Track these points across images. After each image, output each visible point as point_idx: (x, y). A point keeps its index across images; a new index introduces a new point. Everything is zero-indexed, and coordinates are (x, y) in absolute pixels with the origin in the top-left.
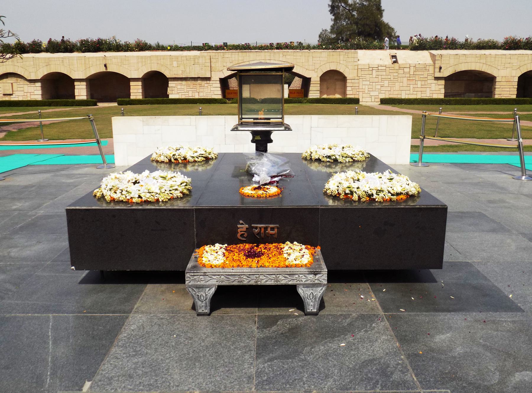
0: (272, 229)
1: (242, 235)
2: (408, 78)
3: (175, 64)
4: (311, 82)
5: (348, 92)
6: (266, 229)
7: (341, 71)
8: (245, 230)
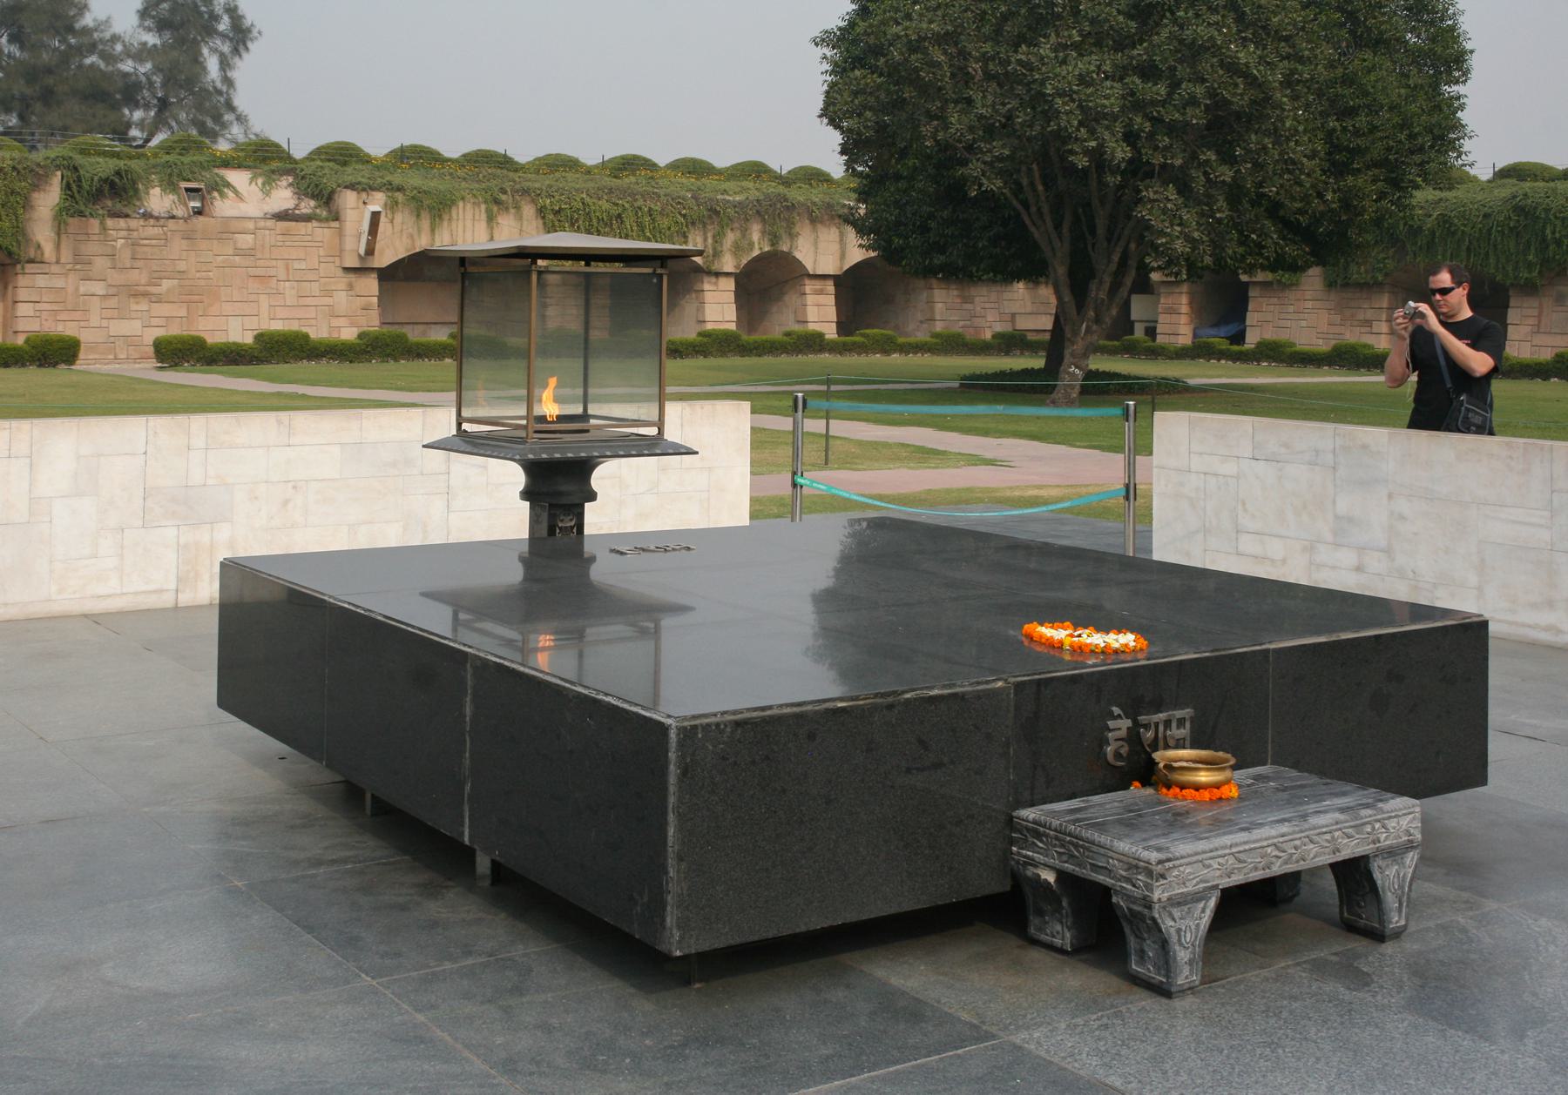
0: (1181, 722)
1: (1118, 755)
2: (252, 271)
6: (1167, 723)
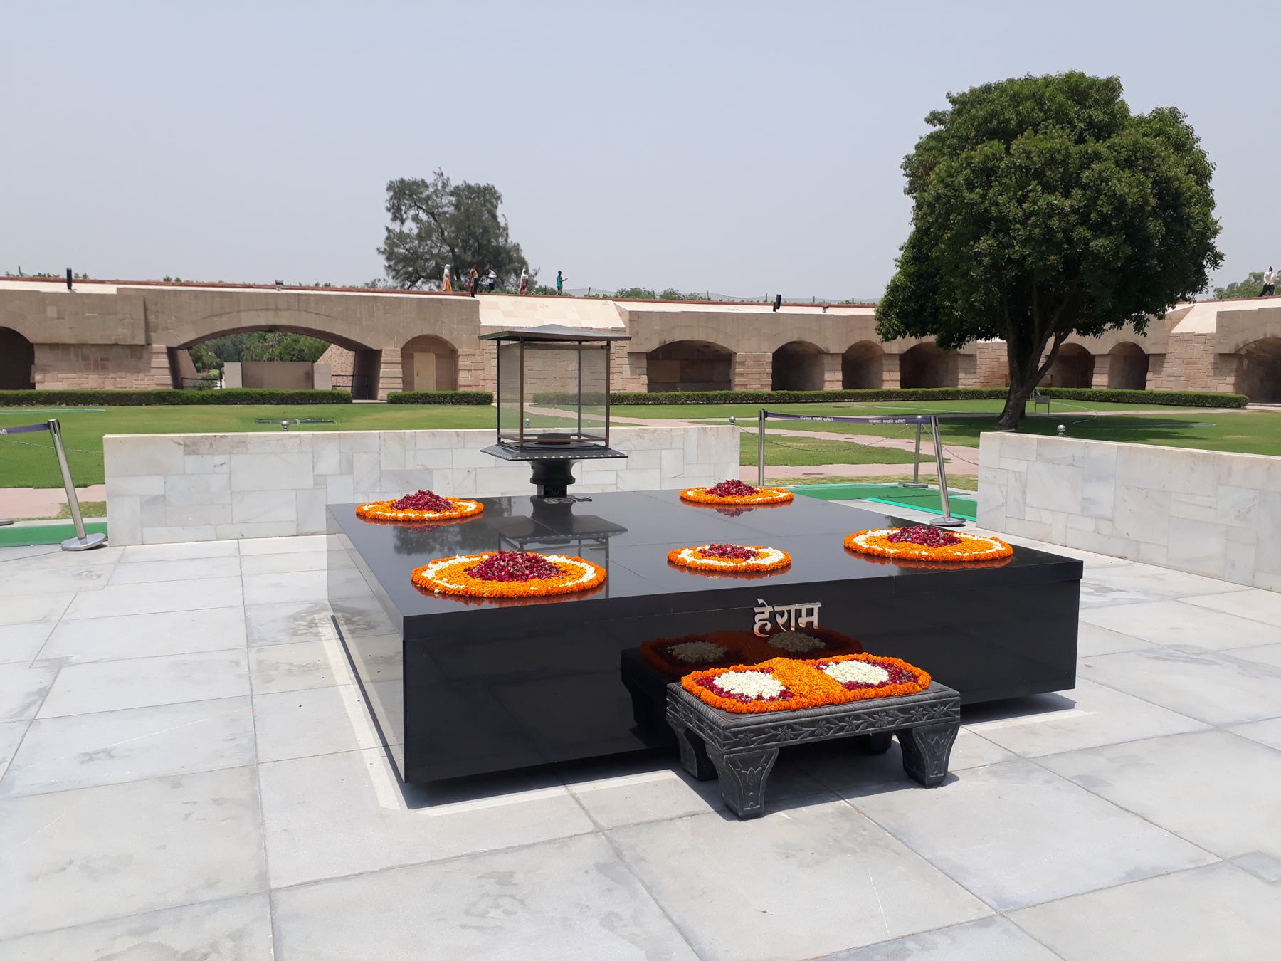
1: (762, 629)
3: (51, 311)
4: (383, 360)
5: (461, 381)
6: (798, 613)
7: (445, 336)
8: (767, 615)
